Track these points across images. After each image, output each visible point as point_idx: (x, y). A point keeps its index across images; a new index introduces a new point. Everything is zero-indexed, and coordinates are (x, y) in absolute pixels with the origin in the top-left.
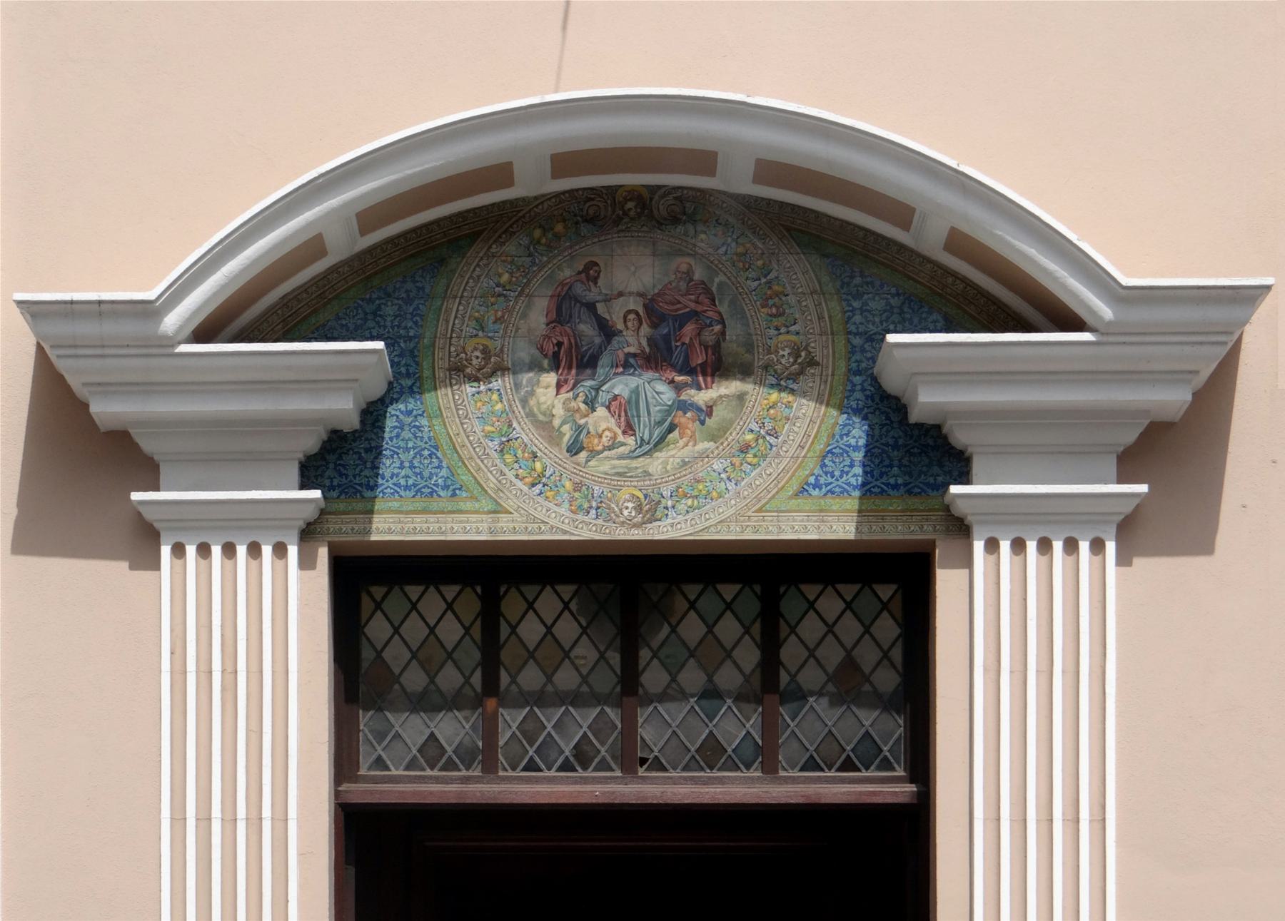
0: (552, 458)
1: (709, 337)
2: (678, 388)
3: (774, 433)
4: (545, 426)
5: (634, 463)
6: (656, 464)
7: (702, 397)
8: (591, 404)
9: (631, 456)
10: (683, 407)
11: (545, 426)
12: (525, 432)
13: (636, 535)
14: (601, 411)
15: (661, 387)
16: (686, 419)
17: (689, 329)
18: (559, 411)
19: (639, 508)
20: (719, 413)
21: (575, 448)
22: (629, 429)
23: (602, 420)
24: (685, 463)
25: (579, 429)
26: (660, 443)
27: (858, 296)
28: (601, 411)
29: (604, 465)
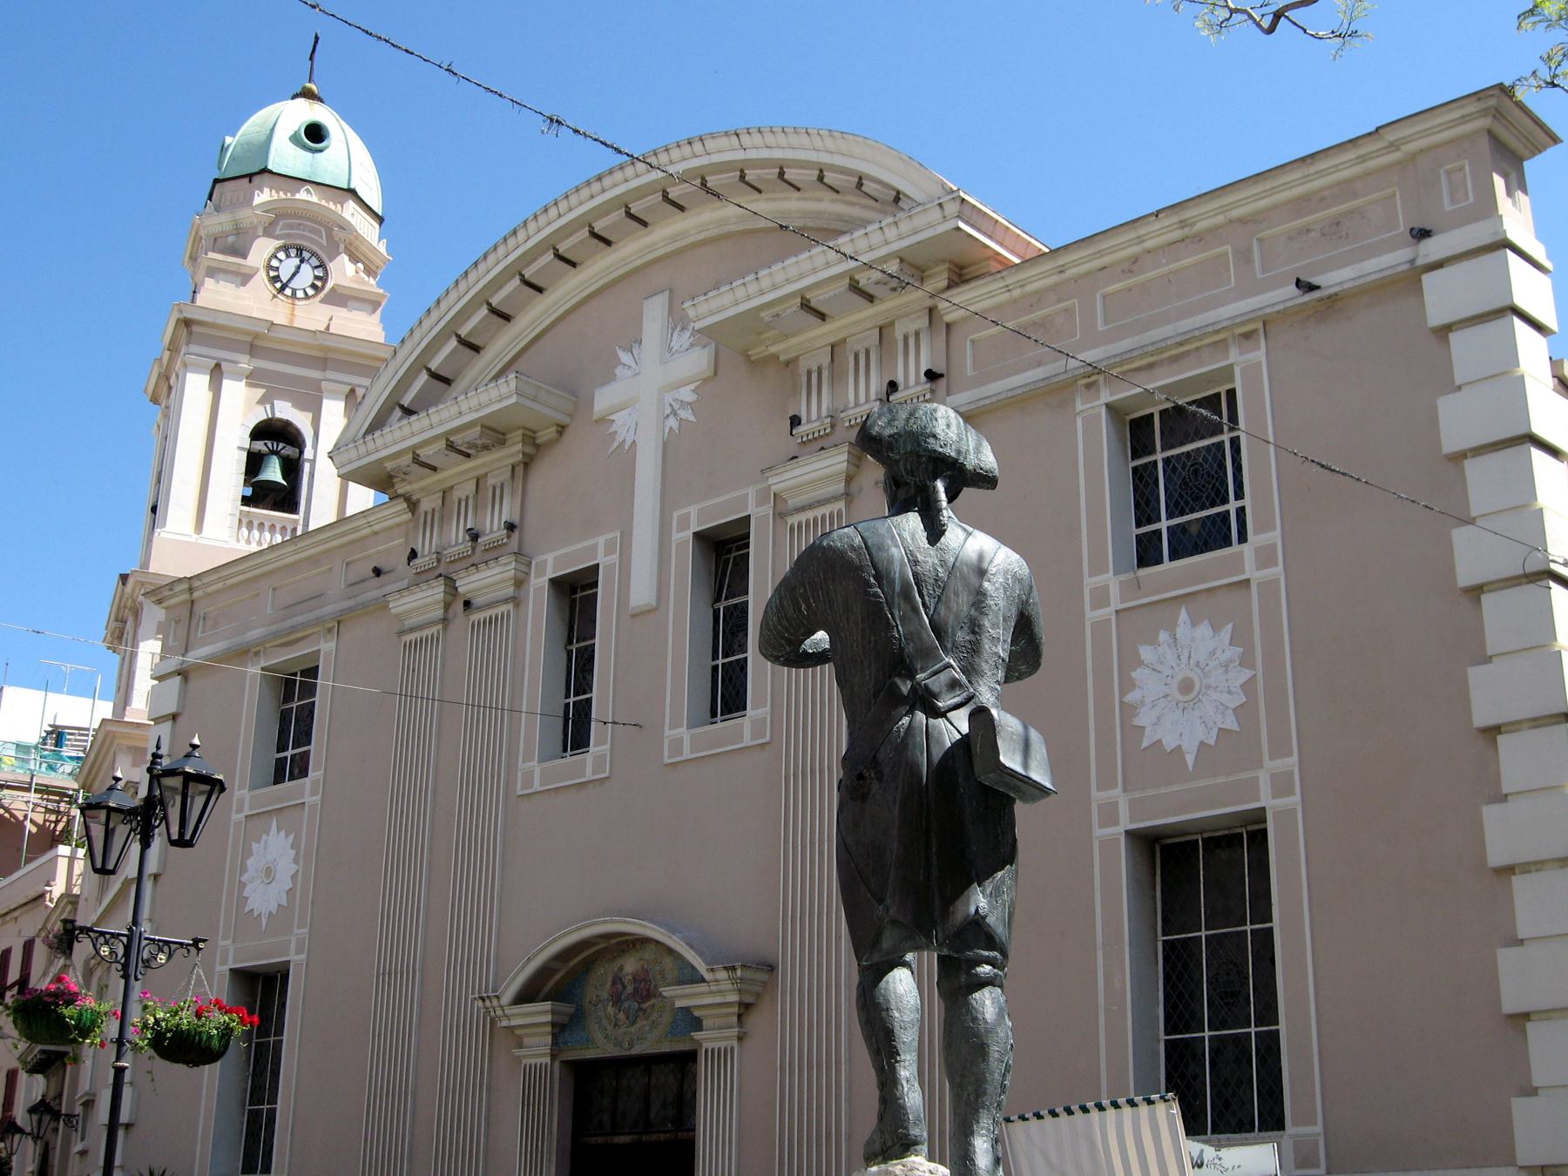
0: (610, 1028)
1: (647, 986)
2: (639, 1003)
3: (661, 1017)
4: (609, 1020)
5: (629, 1029)
6: (633, 1029)
7: (645, 1006)
8: (620, 1011)
9: (627, 1027)
10: (640, 1009)
11: (608, 1017)
12: (605, 1022)
13: (627, 1053)
14: (622, 1013)
15: (635, 1003)
16: (640, 1014)
17: (642, 984)
18: (612, 1014)
19: (629, 1044)
20: (649, 1011)
21: (616, 1025)
22: (627, 1018)
23: (621, 1016)
24: (639, 1029)
25: (617, 1019)
26: (634, 1023)
27: (681, 969)
28: (622, 1013)
29: (623, 1030)
